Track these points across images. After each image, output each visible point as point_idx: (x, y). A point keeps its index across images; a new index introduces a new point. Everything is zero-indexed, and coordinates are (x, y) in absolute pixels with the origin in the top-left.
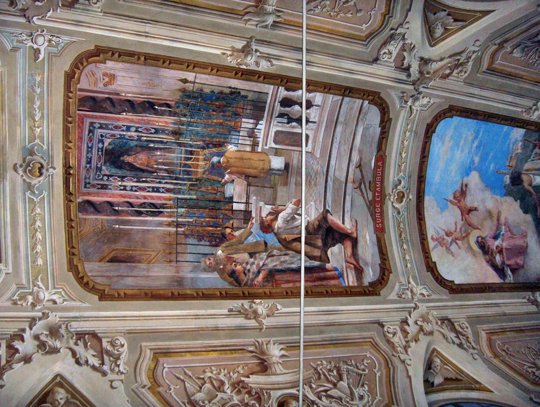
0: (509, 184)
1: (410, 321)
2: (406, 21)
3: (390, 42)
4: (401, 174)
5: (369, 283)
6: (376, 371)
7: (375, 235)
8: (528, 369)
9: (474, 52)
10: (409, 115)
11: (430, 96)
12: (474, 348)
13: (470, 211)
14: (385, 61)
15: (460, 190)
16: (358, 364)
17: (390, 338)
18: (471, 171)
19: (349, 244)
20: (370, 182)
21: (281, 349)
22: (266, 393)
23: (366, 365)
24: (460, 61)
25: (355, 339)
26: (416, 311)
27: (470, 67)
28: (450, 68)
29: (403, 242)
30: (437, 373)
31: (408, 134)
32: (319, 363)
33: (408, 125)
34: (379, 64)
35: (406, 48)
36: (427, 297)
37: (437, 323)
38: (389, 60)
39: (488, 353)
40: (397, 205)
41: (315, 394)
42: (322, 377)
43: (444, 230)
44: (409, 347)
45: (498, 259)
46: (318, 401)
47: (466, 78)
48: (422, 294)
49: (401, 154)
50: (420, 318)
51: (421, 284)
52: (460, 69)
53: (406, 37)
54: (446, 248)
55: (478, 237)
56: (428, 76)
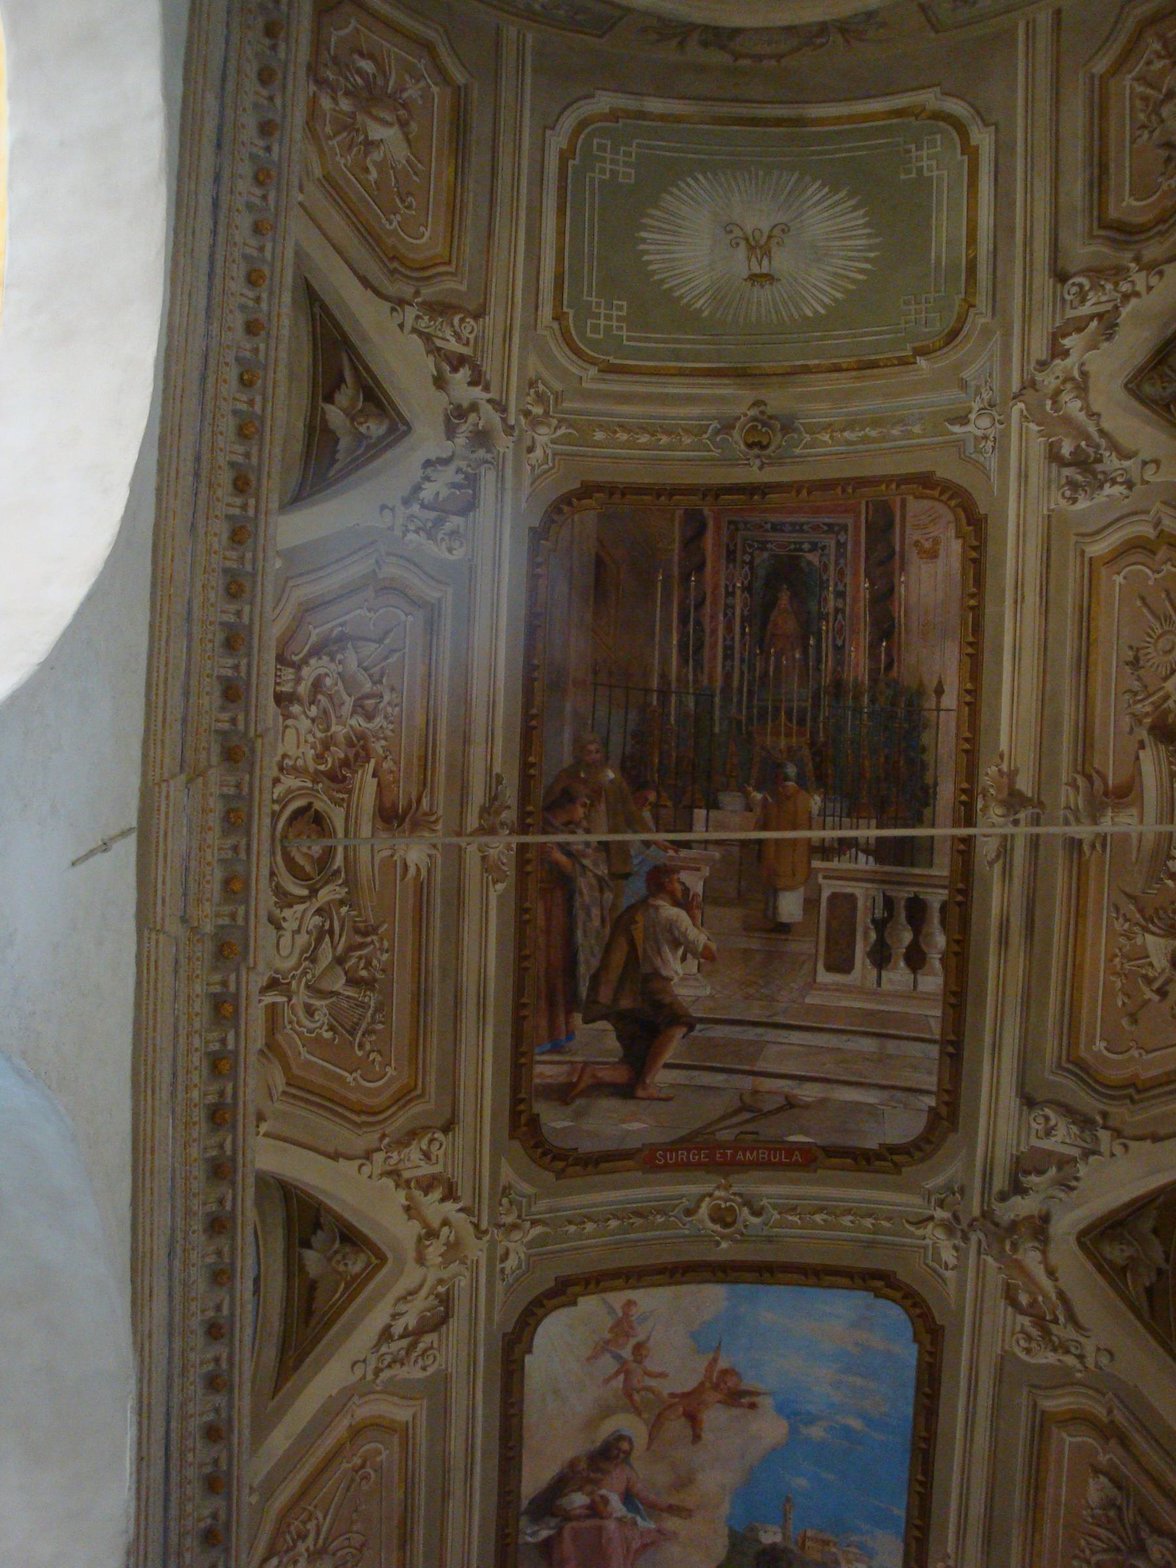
0: (758, 1541)
1: (450, 1207)
2: (1127, 1141)
3: (1074, 1123)
4: (776, 1216)
5: (538, 1115)
6: (357, 1075)
7: (639, 1145)
8: (314, 1522)
9: (1081, 1357)
10: (911, 1220)
11: (961, 1267)
12: (377, 1371)
13: (693, 1419)
14: (1030, 1127)
15: (743, 1387)
16: (374, 1037)
17: (420, 1140)
18: (788, 1417)
19: (620, 1075)
20: (757, 1133)
21: (418, 869)
22: (343, 799)
23: (371, 1058)
24: (1053, 1327)
25: (424, 1047)
26: (471, 1229)
27: (1044, 1361)
28: (1033, 1303)
29: (622, 1219)
30: (330, 1259)
31: (868, 1222)
32: (386, 944)
33: (888, 1219)
34: (1021, 1115)
35: (1067, 1168)
36: (499, 1267)
37: (441, 1281)
38: (1033, 1133)
39: (364, 1411)
40: (704, 1210)
41: (328, 903)
42: (359, 939)
43: (648, 1338)
44: (397, 1186)
45: (578, 1500)
46: (317, 904)
47: (1014, 1355)
48: (505, 1257)
49: (821, 1210)
50: (456, 1236)
51: (529, 1256)
52: (1034, 1332)
53: (1092, 1159)
54: (608, 1342)
55: (630, 1441)
56: (1008, 1247)
